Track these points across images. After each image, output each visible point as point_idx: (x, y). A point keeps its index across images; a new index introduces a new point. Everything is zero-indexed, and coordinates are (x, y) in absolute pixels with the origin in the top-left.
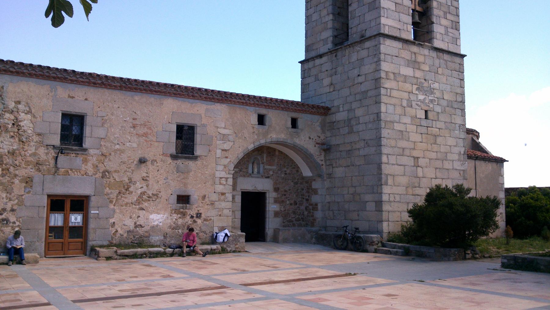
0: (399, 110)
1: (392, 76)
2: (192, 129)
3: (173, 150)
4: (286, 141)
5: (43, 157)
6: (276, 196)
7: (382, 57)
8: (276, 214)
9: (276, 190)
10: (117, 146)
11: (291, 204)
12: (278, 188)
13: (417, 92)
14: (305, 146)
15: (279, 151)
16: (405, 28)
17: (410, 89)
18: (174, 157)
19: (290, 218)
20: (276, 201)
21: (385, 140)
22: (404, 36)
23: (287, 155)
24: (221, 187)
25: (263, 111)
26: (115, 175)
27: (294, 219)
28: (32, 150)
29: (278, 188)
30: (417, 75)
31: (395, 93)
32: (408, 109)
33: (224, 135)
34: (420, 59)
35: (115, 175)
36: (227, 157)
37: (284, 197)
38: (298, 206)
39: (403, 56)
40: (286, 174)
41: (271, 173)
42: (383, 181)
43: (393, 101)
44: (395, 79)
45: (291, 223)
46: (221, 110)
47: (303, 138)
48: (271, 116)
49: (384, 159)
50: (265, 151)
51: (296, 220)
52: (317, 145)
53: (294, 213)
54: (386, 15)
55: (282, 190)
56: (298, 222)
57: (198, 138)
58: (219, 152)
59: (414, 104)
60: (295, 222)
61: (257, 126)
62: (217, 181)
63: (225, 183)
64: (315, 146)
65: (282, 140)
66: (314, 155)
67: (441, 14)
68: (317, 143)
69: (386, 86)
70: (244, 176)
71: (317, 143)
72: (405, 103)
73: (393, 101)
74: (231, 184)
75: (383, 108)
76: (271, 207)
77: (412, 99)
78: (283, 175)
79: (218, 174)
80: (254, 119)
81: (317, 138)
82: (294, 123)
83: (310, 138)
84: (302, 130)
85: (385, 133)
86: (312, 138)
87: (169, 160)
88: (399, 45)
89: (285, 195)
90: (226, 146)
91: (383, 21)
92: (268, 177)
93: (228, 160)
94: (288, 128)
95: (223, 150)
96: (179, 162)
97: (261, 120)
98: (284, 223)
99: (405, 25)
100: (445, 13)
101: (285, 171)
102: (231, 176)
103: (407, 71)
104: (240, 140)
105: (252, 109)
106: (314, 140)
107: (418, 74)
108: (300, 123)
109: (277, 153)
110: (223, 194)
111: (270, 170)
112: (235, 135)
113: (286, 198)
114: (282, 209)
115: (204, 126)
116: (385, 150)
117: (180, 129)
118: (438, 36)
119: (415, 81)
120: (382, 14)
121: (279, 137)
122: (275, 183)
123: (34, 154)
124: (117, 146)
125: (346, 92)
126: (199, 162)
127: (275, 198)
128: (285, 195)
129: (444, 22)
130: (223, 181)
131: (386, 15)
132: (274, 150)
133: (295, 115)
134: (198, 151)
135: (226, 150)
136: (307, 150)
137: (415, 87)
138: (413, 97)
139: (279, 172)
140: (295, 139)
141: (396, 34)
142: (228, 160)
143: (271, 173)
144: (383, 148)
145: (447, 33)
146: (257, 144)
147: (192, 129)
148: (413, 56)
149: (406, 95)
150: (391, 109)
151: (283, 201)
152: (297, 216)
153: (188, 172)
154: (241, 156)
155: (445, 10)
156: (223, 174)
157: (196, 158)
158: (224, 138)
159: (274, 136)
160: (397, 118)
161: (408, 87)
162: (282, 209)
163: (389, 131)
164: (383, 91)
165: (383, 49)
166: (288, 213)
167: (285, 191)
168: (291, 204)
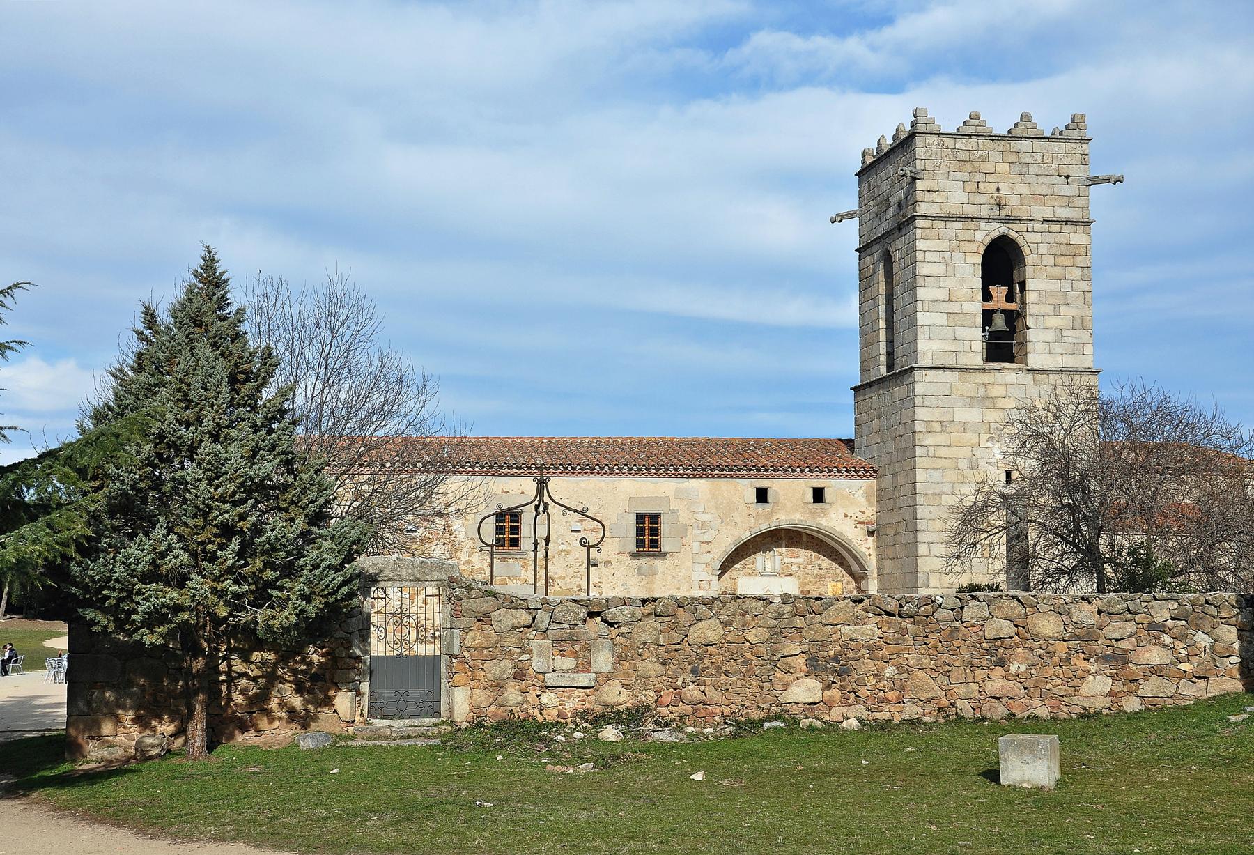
0: (952, 475)
1: (937, 427)
2: (655, 518)
3: (632, 546)
5: (477, 565)
7: (918, 400)
10: (562, 547)
13: (989, 444)
16: (967, 348)
17: (975, 441)
18: (634, 556)
21: (924, 522)
22: (964, 361)
25: (763, 483)
26: (561, 582)
28: (465, 558)
30: (987, 419)
31: (942, 452)
32: (969, 473)
34: (996, 391)
35: (561, 582)
39: (960, 393)
42: (920, 581)
43: (941, 463)
44: (943, 431)
46: (699, 486)
48: (776, 486)
49: (922, 549)
54: (927, 336)
57: (665, 529)
58: (696, 545)
59: (982, 463)
62: (696, 585)
67: (1049, 309)
69: (926, 443)
72: (963, 464)
73: (941, 463)
75: (920, 476)
77: (978, 456)
79: (696, 576)
81: (859, 514)
82: (819, 495)
83: (846, 516)
84: (832, 504)
85: (921, 512)
87: (628, 559)
88: (954, 376)
90: (706, 538)
91: (921, 345)
96: (642, 561)
97: (762, 495)
99: (967, 344)
100: (1057, 307)
103: (974, 415)
105: (746, 481)
107: (991, 416)
108: (828, 495)
109: (804, 538)
115: (674, 511)
116: (920, 537)
117: (640, 517)
118: (1039, 347)
119: (985, 427)
120: (920, 335)
123: (468, 562)
124: (562, 547)
125: (890, 446)
126: (668, 561)
129: (1054, 321)
130: (705, 585)
131: (927, 336)
132: (800, 534)
133: (818, 483)
134: (666, 545)
135: (707, 543)
137: (984, 437)
138: (978, 453)
141: (950, 362)
143: (795, 568)
144: (919, 534)
145: (1059, 338)
146: (756, 531)
147: (655, 518)
148: (982, 390)
149: (966, 452)
150: (936, 475)
153: (654, 574)
154: (731, 549)
155: (1056, 302)
156: (704, 576)
157: (665, 555)
158: (704, 526)
160: (947, 489)
161: (971, 438)
163: (931, 508)
164: (919, 451)
165: (919, 388)
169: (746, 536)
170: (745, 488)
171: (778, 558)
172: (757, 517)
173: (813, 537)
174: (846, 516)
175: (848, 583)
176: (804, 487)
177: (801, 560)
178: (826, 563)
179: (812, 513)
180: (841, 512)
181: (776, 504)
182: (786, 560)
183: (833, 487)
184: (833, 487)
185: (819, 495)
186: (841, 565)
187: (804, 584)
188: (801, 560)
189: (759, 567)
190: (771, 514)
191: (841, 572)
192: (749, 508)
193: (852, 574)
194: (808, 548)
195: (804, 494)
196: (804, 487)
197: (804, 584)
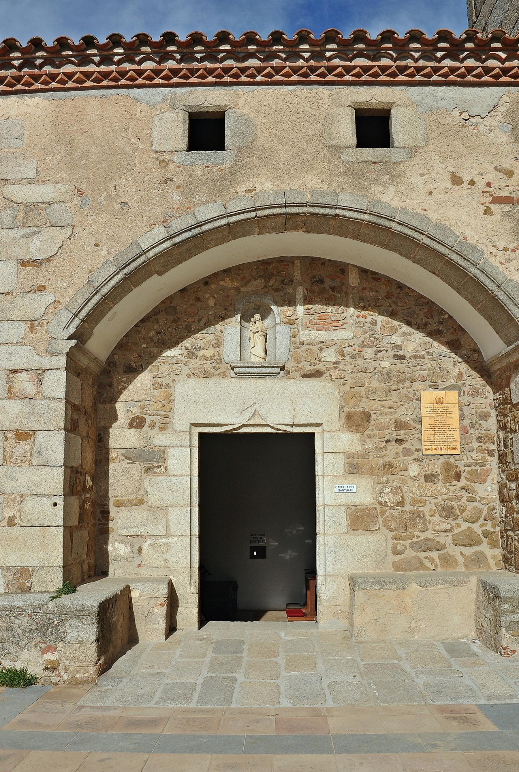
4: (329, 200)
6: (356, 447)
8: (360, 519)
9: (357, 421)
11: (429, 478)
12: (367, 417)
14: (434, 216)
15: (363, 272)
19: (429, 534)
20: (354, 467)
23: (400, 286)
24: (15, 407)
25: (209, 98)
27: (446, 539)
29: (367, 417)
33: (31, 206)
36: (41, 289)
37: (392, 447)
38: (463, 482)
40: (402, 358)
41: (330, 356)
45: (435, 555)
47: (417, 181)
48: (244, 105)
50: (298, 276)
51: (457, 543)
52: (494, 207)
53: (448, 512)
55: (384, 420)
56: (468, 551)
60: (453, 550)
61: (183, 157)
63: (31, 389)
64: (488, 212)
65: (308, 198)
66: (487, 250)
68: (498, 200)
70: (207, 375)
71: (498, 200)
74: (61, 392)
76: (334, 492)
78: (386, 364)
80: (174, 131)
81: (492, 176)
82: (373, 128)
83: (456, 180)
84: (413, 151)
86: (466, 177)
89: (399, 441)
90: (36, 248)
92: (318, 374)
93: (48, 298)
94: (337, 149)
95: (24, 263)
97: (206, 132)
98: (396, 552)
101: (399, 347)
102: (63, 361)
104: (102, 218)
106: (481, 184)
108: (399, 128)
109: (353, 280)
110: (22, 435)
111: (323, 345)
112: (77, 199)
113: (407, 452)
114: (388, 498)
121: (294, 185)
122: (348, 397)
127: (349, 455)
128: (399, 441)
130: (25, 383)
133: (372, 96)
135: (37, 263)
136: (446, 229)
139: (369, 352)
140: (374, 189)
142: (48, 298)
143: (330, 356)
151: (389, 466)
152: (465, 526)
156: (24, 356)
159: (268, 186)
162: (388, 498)
166: (417, 516)
167: (400, 425)
168: (429, 478)
169: (153, 238)
170: (160, 114)
171: (283, 331)
172: (188, 189)
173: (375, 276)
174: (456, 180)
175: (475, 393)
176: (336, 107)
177: (344, 334)
178: (414, 341)
179: (356, 175)
180: (442, 170)
181: (247, 149)
182: (304, 335)
183: (409, 107)
184: (409, 107)
185: (373, 128)
186: (454, 346)
187: (358, 398)
188: (344, 334)
189: (231, 353)
190: (231, 177)
191: (454, 365)
192: (163, 164)
193: (484, 370)
194: (363, 303)
195: (328, 122)
196: (336, 107)
197: (358, 398)
